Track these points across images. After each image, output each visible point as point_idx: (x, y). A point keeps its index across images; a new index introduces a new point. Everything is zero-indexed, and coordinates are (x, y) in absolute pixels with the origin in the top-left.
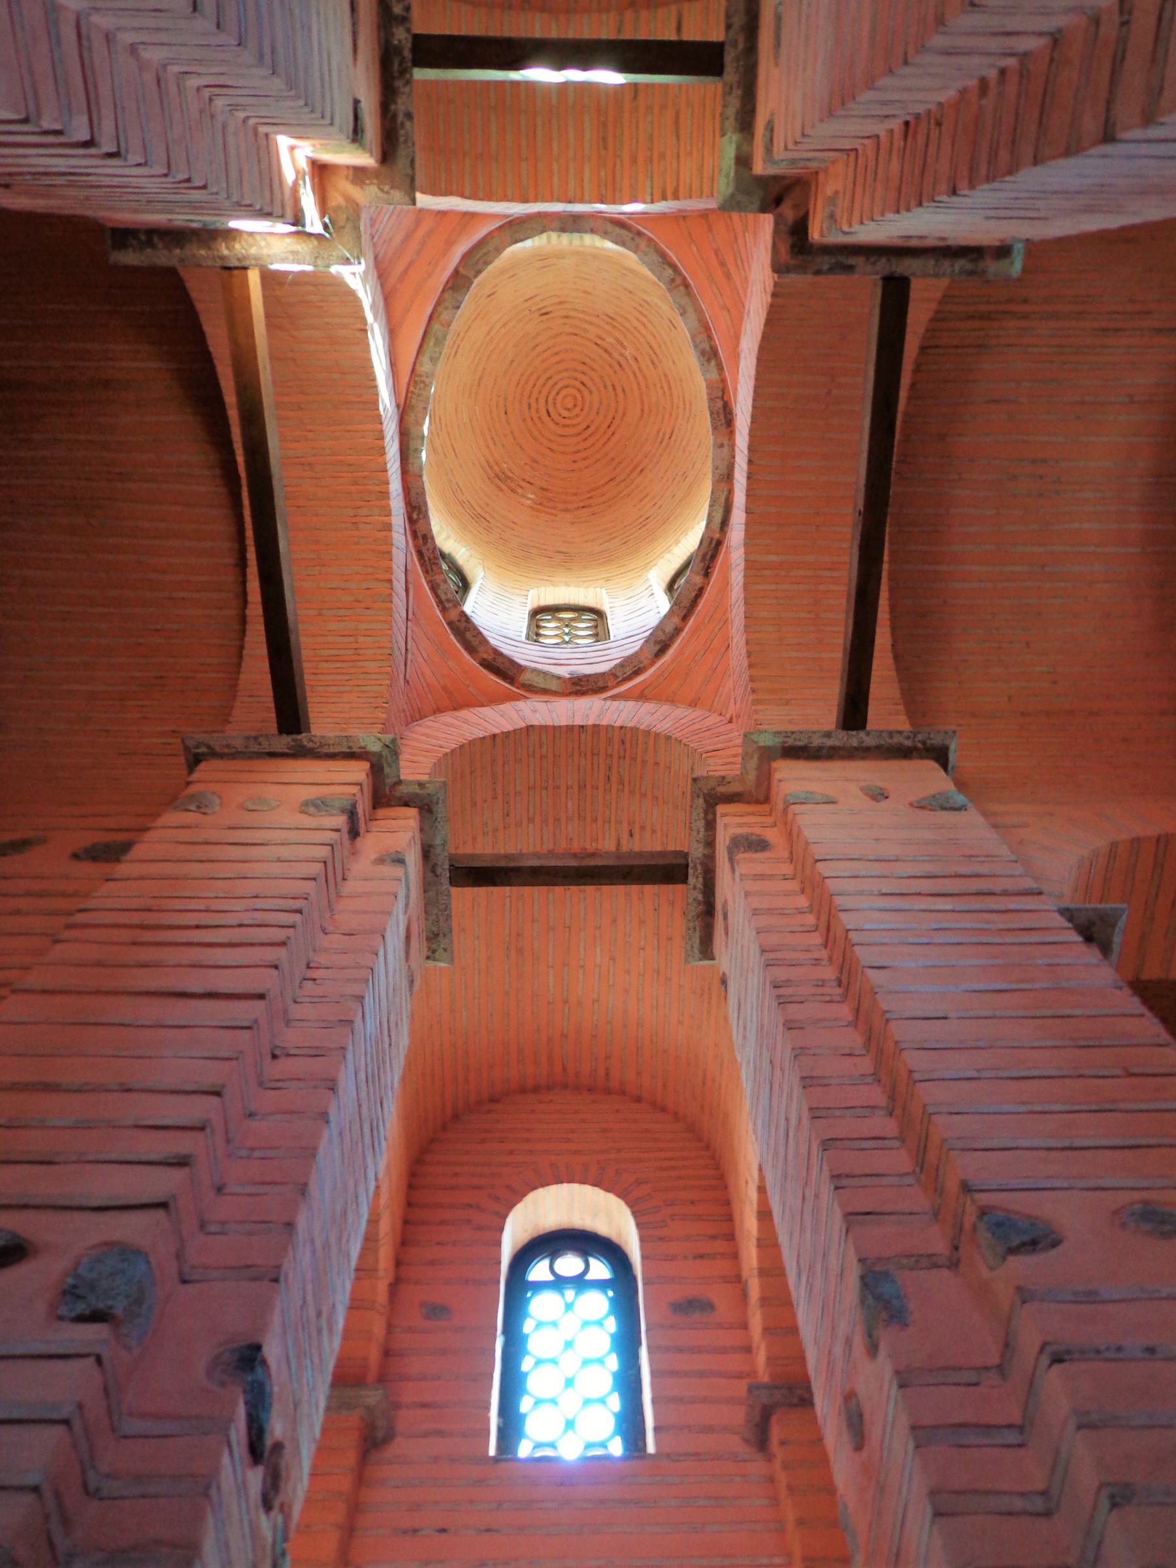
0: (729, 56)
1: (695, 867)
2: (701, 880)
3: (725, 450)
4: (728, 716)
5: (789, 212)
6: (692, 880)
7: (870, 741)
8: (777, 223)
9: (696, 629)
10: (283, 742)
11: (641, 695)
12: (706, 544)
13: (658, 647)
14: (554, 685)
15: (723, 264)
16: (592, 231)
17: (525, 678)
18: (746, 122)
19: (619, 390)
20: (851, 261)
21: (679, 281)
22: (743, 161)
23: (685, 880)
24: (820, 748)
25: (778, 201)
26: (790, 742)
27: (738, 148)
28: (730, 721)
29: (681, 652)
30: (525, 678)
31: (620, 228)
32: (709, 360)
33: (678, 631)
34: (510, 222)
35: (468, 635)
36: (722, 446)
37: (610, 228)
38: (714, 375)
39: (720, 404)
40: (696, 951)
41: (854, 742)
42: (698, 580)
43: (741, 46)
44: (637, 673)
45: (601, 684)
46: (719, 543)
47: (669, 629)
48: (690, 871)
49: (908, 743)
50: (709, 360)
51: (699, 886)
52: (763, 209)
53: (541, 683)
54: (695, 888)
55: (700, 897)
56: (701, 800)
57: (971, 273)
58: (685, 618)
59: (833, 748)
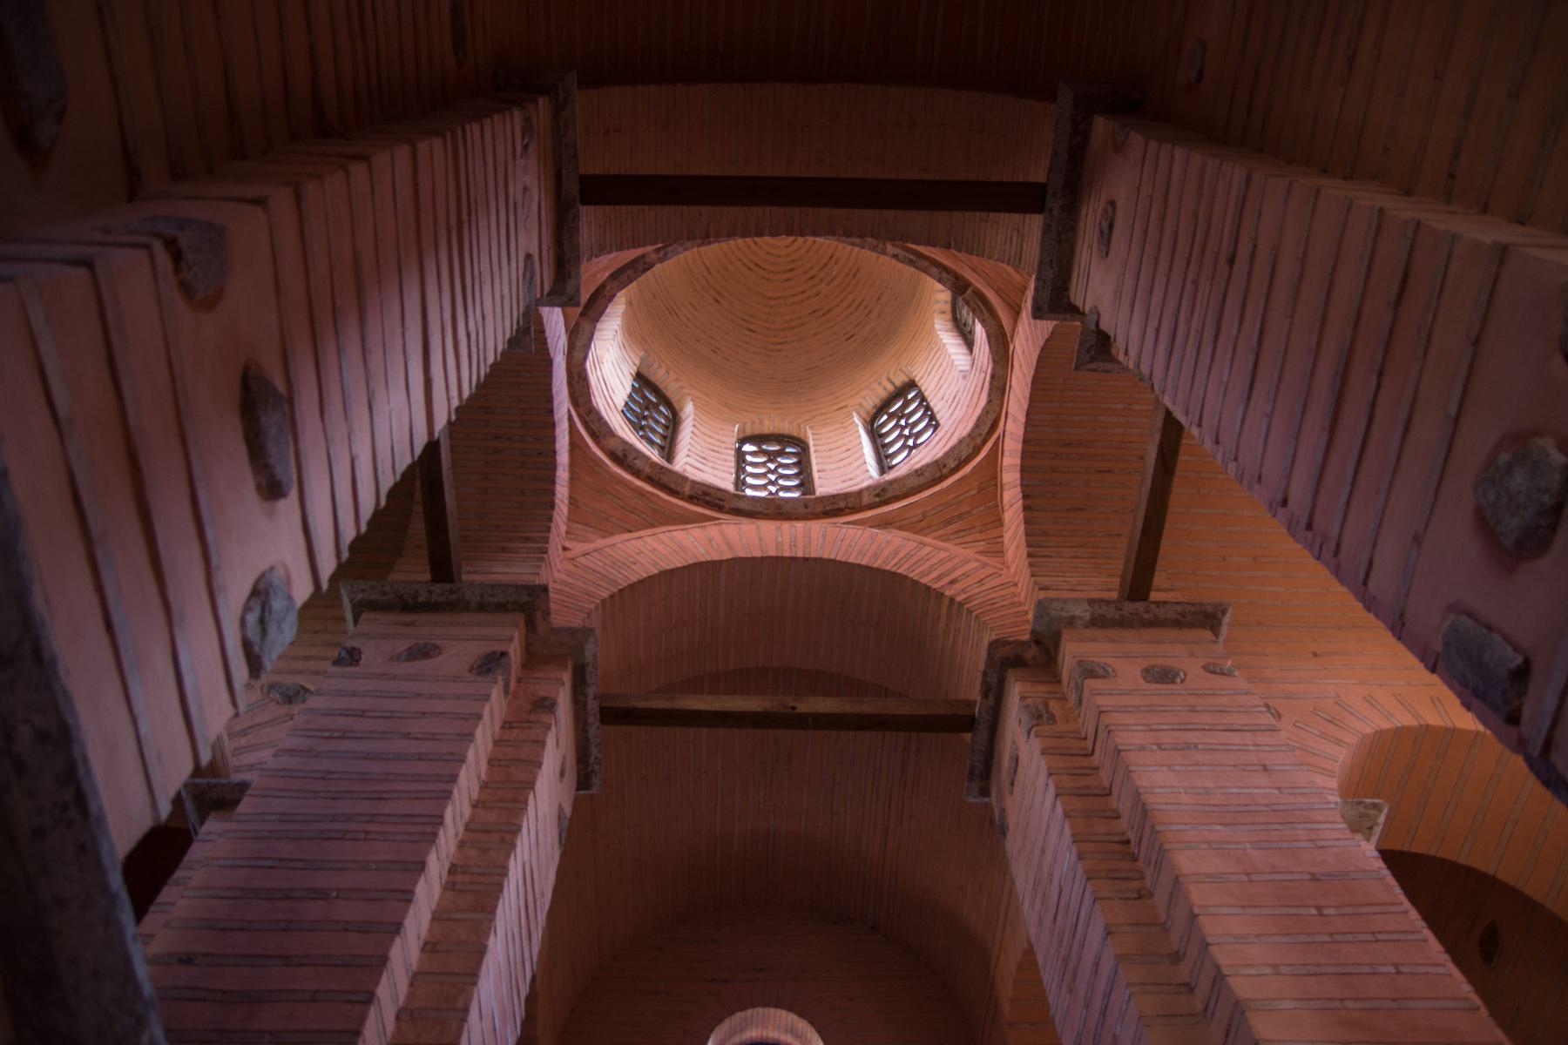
0: (1139, 606)
1: (452, 592)
2: (441, 599)
3: (802, 511)
4: (567, 544)
5: (1032, 652)
6: (438, 588)
7: (592, 731)
8: (1023, 643)
9: (639, 491)
10: (572, 187)
11: (576, 445)
12: (720, 495)
13: (620, 454)
14: (577, 355)
15: (960, 517)
16: (989, 402)
17: (586, 326)
18: (1098, 622)
19: (789, 275)
20: (991, 697)
21: (945, 471)
22: (1071, 621)
23: (435, 580)
24: (584, 694)
25: (1038, 642)
26: (589, 669)
27: (1081, 618)
28: (565, 549)
29: (621, 481)
30: (586, 326)
31: (989, 422)
32: (878, 495)
33: (636, 473)
34: (1004, 334)
35: (629, 272)
36: (806, 507)
37: (992, 417)
38: (866, 500)
39: (842, 505)
40: (360, 596)
41: (591, 719)
42: (687, 490)
43: (1146, 616)
44: (595, 436)
45: (581, 400)
46: (720, 509)
47: (638, 463)
48: (448, 586)
49: (592, 760)
50: (878, 495)
51: (434, 598)
52: (1033, 632)
53: (579, 343)
54: (430, 592)
55: (420, 599)
56: (526, 598)
57: (971, 772)
58: (649, 480)
59: (585, 704)
